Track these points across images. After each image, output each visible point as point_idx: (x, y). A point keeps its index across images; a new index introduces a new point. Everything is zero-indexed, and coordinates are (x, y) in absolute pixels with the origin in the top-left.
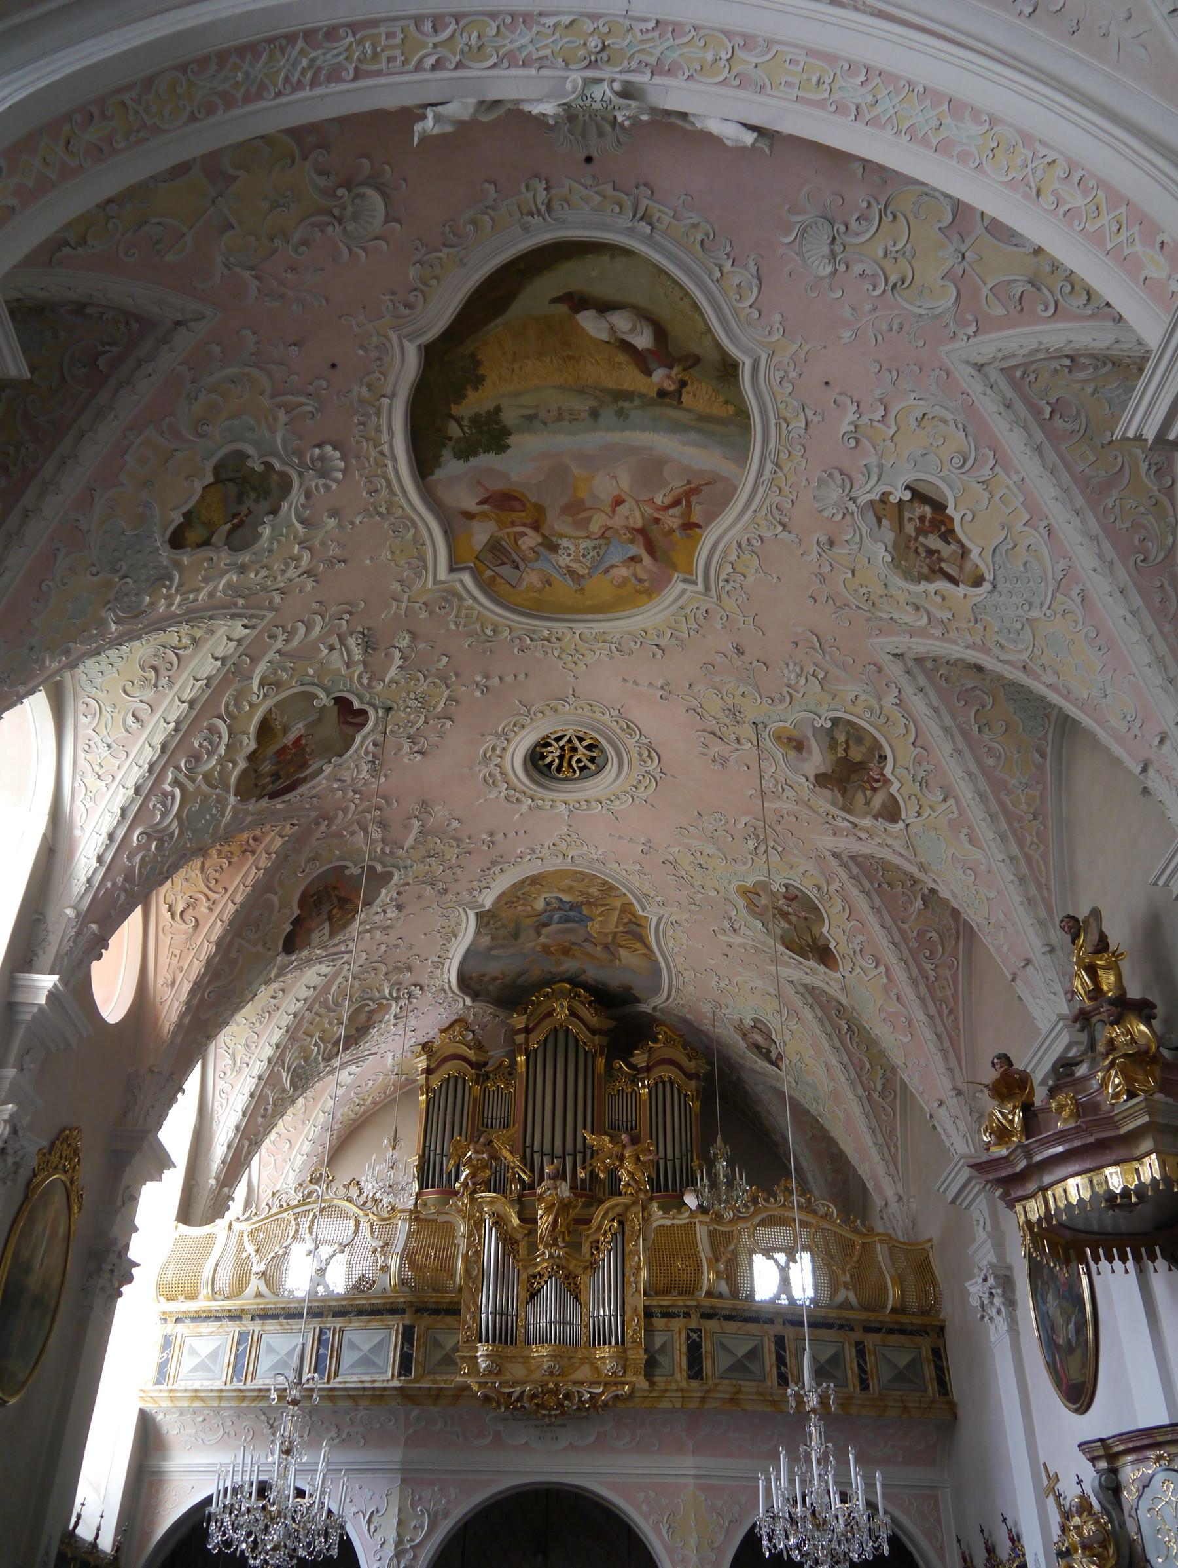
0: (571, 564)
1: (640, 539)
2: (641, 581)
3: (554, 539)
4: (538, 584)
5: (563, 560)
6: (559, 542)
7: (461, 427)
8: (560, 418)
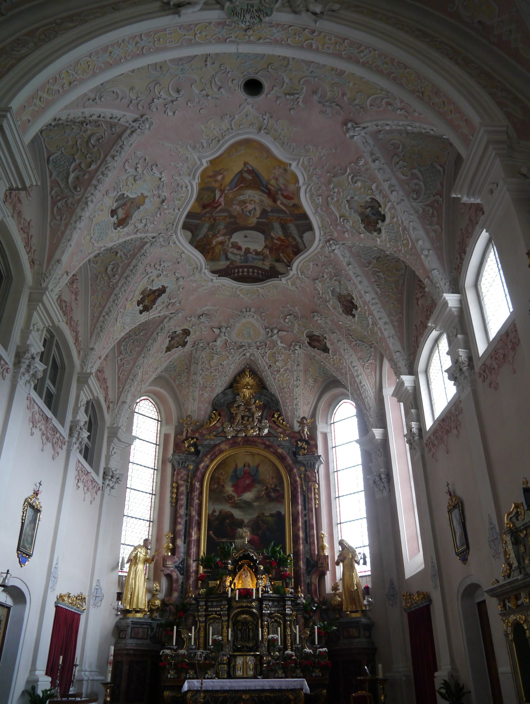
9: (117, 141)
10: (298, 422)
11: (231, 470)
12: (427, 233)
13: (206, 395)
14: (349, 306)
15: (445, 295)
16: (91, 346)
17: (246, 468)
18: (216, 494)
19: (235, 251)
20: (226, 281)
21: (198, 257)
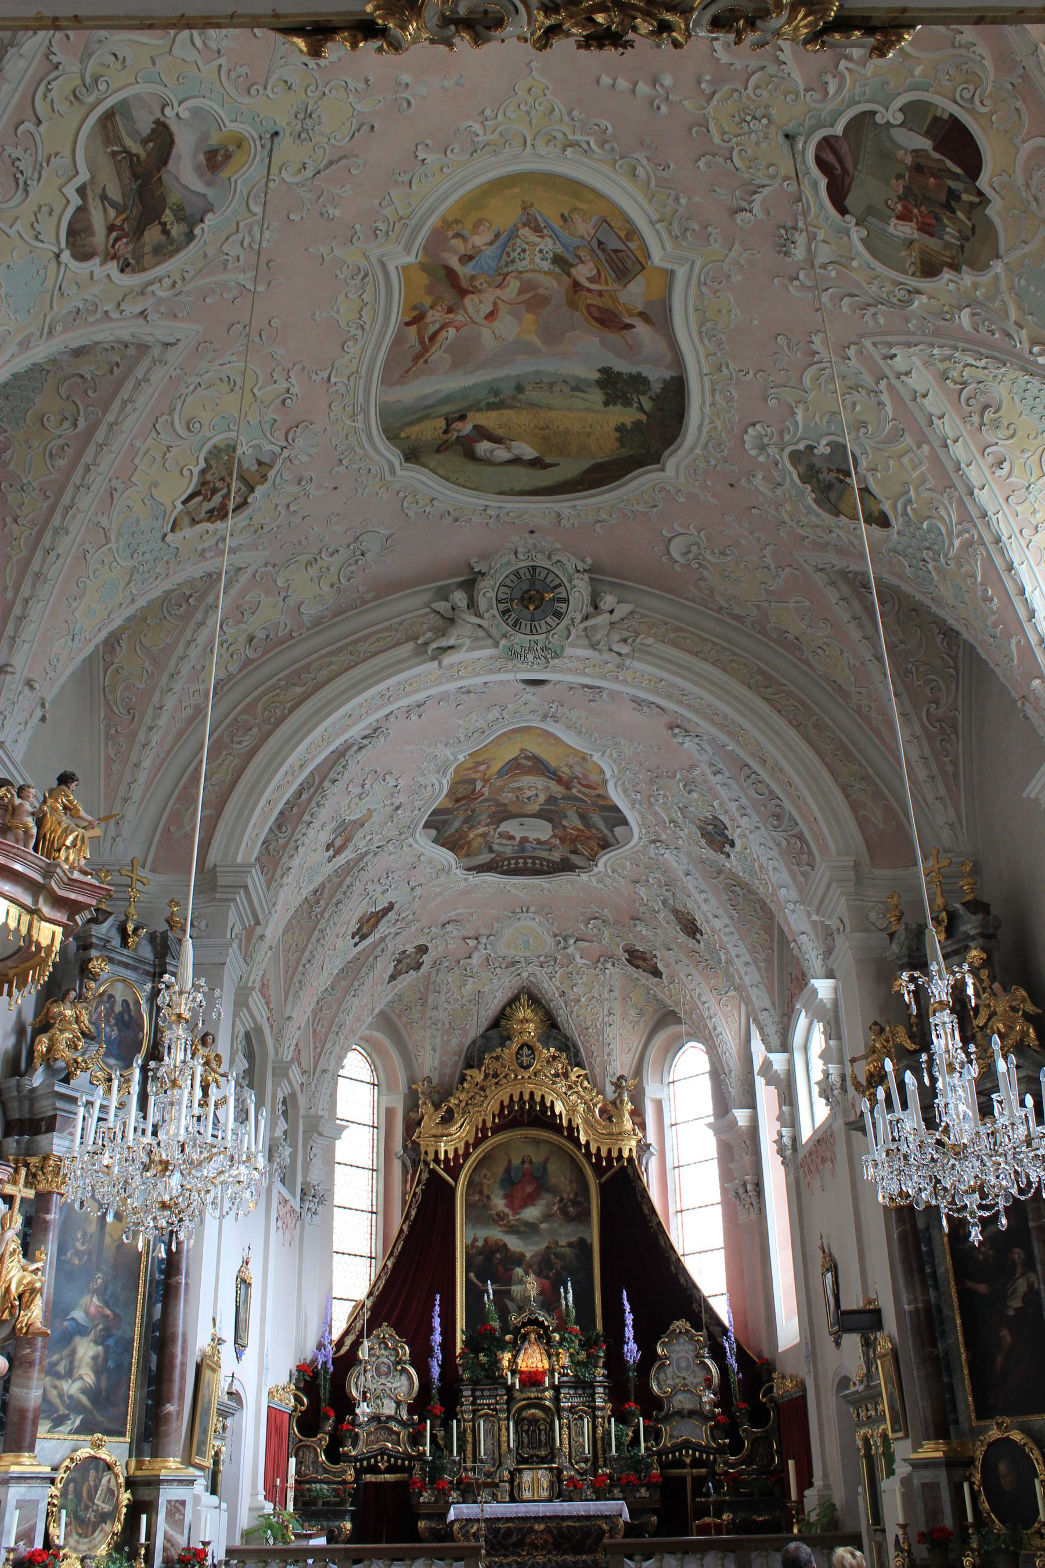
0: (538, 240)
1: (464, 284)
2: (457, 235)
3: (558, 270)
4: (577, 218)
5: (548, 245)
6: (552, 267)
7: (640, 403)
8: (551, 385)
9: (338, 759)
10: (612, 1083)
11: (500, 1170)
12: (794, 878)
13: (454, 1042)
14: (692, 929)
15: (813, 981)
16: (287, 1014)
17: (527, 1166)
18: (478, 1212)
19: (504, 841)
20: (491, 878)
21: (446, 856)
